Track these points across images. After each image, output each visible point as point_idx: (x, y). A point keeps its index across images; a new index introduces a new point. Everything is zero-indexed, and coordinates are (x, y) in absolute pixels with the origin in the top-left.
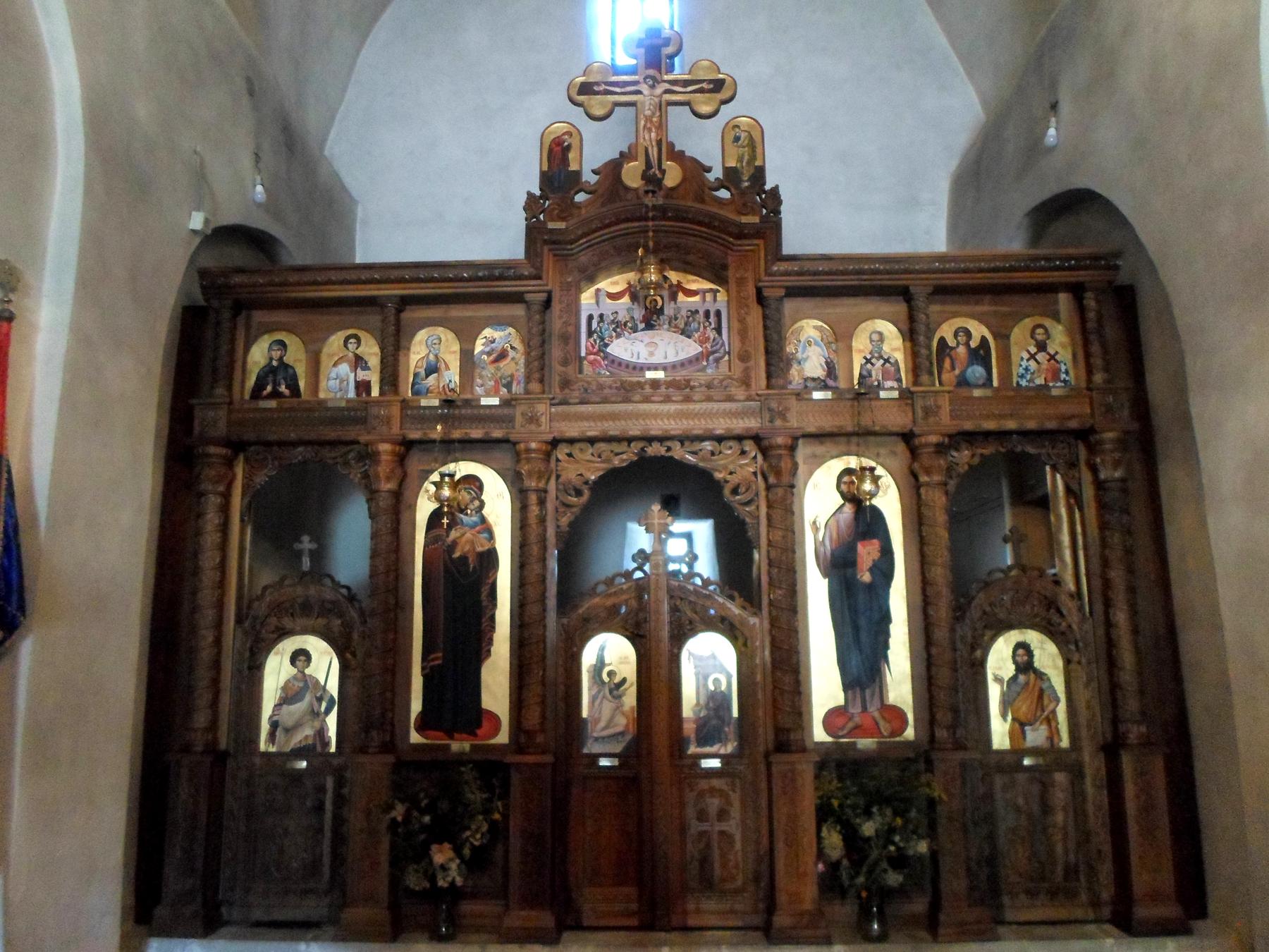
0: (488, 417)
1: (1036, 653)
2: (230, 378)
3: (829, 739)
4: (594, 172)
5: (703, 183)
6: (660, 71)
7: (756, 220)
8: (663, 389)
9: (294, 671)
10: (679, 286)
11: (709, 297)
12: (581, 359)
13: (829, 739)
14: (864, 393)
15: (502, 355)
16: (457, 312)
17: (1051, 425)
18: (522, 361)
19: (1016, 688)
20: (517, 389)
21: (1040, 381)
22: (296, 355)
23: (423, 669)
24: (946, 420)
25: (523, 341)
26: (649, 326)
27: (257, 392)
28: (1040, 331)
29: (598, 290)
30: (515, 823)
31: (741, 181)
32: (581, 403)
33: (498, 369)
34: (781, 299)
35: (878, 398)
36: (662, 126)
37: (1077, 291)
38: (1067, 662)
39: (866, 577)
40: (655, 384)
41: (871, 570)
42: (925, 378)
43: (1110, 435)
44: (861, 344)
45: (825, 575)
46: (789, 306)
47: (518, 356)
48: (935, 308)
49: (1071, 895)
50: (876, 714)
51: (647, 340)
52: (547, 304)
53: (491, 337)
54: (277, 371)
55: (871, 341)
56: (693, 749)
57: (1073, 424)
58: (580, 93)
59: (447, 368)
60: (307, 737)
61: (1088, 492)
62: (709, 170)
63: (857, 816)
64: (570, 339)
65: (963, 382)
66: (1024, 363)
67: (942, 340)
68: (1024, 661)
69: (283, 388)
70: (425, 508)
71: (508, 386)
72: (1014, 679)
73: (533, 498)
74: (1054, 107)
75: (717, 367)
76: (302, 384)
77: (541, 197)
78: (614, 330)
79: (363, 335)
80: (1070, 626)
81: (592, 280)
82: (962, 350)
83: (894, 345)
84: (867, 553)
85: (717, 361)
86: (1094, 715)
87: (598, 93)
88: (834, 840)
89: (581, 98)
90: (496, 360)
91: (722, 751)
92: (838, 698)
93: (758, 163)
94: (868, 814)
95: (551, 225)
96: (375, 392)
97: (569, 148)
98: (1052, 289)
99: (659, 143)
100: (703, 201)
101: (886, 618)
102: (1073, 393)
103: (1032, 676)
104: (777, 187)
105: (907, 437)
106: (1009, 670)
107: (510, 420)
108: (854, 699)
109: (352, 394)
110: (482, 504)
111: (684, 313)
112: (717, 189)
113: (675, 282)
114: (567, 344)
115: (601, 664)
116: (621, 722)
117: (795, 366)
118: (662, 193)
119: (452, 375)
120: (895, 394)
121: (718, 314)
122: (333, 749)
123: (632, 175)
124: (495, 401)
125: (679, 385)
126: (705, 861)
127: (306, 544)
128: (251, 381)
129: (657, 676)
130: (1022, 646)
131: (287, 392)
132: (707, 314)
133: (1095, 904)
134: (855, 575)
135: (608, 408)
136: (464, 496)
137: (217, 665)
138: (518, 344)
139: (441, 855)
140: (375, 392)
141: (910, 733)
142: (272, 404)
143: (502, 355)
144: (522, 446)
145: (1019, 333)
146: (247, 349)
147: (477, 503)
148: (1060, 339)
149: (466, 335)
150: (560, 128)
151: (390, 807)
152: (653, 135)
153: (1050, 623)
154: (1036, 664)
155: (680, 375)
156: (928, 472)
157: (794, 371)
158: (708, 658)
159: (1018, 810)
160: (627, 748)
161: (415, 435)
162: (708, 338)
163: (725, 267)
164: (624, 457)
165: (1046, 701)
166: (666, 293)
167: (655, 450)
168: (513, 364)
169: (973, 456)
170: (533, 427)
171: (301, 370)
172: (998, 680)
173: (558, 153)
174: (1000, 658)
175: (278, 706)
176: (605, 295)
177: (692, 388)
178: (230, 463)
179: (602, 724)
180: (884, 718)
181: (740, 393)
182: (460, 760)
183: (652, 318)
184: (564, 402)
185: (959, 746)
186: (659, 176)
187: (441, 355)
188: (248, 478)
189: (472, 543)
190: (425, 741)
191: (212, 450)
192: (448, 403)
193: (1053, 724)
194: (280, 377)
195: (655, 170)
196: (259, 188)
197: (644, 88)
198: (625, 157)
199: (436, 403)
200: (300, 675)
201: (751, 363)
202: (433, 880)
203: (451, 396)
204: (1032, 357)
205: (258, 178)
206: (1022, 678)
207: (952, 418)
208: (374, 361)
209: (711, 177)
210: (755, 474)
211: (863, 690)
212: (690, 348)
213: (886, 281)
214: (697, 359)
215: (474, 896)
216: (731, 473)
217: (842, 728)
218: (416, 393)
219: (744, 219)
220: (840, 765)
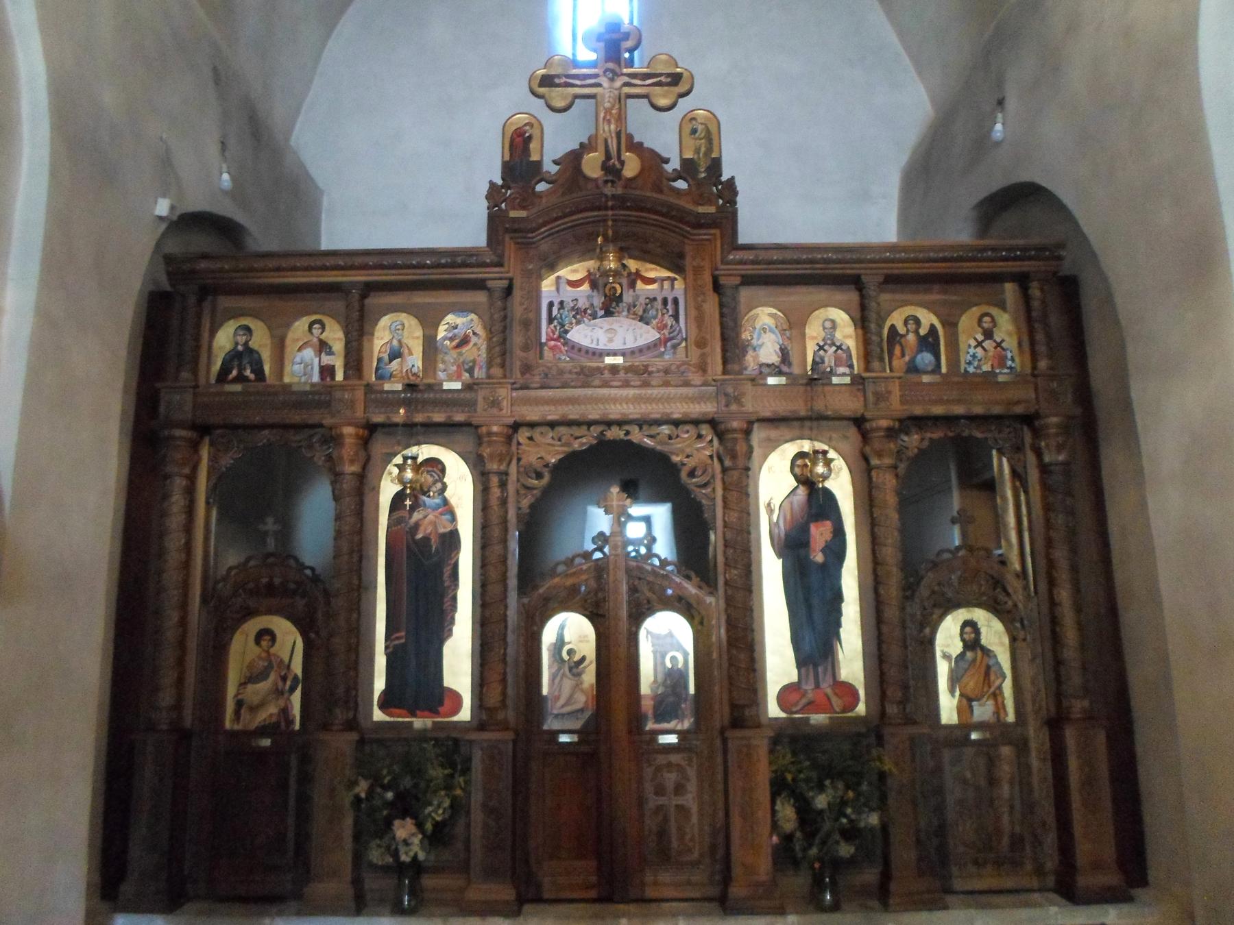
0: (450, 401)
1: (983, 631)
2: (195, 361)
3: (783, 715)
4: (555, 162)
5: (662, 172)
6: (619, 65)
7: (712, 210)
8: (622, 374)
9: (257, 650)
10: (638, 275)
11: (666, 285)
12: (541, 345)
13: (783, 715)
14: (816, 379)
15: (465, 341)
16: (421, 298)
17: (997, 410)
18: (484, 347)
19: (964, 665)
20: (479, 373)
21: (986, 368)
22: (261, 340)
23: (386, 648)
24: (896, 405)
25: (485, 328)
26: (608, 313)
27: (223, 376)
28: (986, 319)
29: (558, 278)
30: (477, 798)
31: (697, 171)
32: (542, 387)
33: (460, 354)
34: (737, 287)
35: (830, 384)
36: (621, 118)
37: (1022, 280)
38: (1013, 640)
39: (819, 558)
40: (614, 369)
41: (823, 551)
42: (876, 364)
43: (1054, 420)
44: (814, 331)
45: (779, 555)
46: (745, 294)
47: (480, 341)
48: (885, 297)
49: (1016, 864)
50: (829, 691)
51: (606, 327)
52: (509, 291)
53: (453, 323)
54: (243, 356)
55: (824, 328)
56: (650, 726)
57: (1019, 410)
58: (541, 84)
59: (411, 353)
60: (271, 715)
61: (1033, 475)
62: (667, 161)
63: (812, 789)
64: (530, 325)
65: (913, 368)
66: (972, 351)
67: (893, 327)
68: (972, 638)
69: (248, 373)
70: (388, 489)
71: (470, 371)
72: (961, 656)
73: (495, 480)
74: (1001, 102)
75: (674, 353)
76: (267, 368)
77: (502, 187)
78: (574, 317)
79: (328, 321)
80: (1015, 605)
81: (552, 267)
82: (911, 337)
83: (847, 333)
84: (820, 533)
85: (675, 347)
86: (1039, 691)
87: (558, 85)
88: (787, 813)
89: (542, 90)
90: (458, 346)
91: (679, 727)
92: (792, 675)
93: (714, 155)
94: (821, 788)
95: (513, 214)
96: (339, 377)
97: (530, 137)
98: (997, 278)
99: (618, 134)
100: (661, 192)
101: (838, 597)
102: (1019, 379)
103: (979, 653)
104: (733, 178)
105: (859, 422)
106: (957, 647)
107: (472, 404)
108: (807, 676)
109: (316, 378)
110: (444, 487)
111: (642, 300)
112: (674, 180)
113: (633, 270)
114: (528, 330)
115: (560, 643)
116: (581, 700)
117: (751, 353)
118: (621, 183)
119: (415, 360)
120: (847, 380)
121: (676, 301)
122: (297, 727)
123: (592, 165)
124: (457, 386)
125: (637, 371)
126: (662, 834)
127: (270, 525)
129: (616, 655)
130: (969, 624)
131: (252, 376)
132: (665, 301)
133: (1039, 871)
134: (807, 556)
135: (569, 392)
136: (426, 478)
137: (182, 644)
138: (479, 330)
139: (403, 829)
140: (339, 377)
141: (861, 708)
142: (238, 388)
143: (465, 341)
144: (484, 430)
145: (967, 321)
147: (439, 485)
148: (1006, 327)
149: (430, 322)
150: (521, 118)
151: (353, 784)
152: (613, 127)
153: (996, 601)
154: (983, 642)
155: (639, 361)
156: (880, 455)
157: (749, 358)
158: (666, 636)
159: (965, 782)
160: (585, 725)
161: (378, 418)
162: (665, 326)
163: (681, 256)
164: (584, 441)
165: (992, 677)
166: (625, 281)
167: (615, 433)
168: (475, 349)
169: (923, 439)
170: (495, 411)
171: (266, 355)
172: (946, 656)
173: (519, 144)
174: (948, 636)
175: (243, 684)
176: (564, 283)
177: (650, 373)
178: (195, 446)
179: (562, 701)
180: (836, 694)
181: (697, 379)
182: (423, 736)
184: (525, 387)
185: (909, 721)
186: (618, 166)
187: (405, 341)
188: (213, 459)
189: (434, 524)
190: (388, 719)
191: (178, 433)
192: (410, 387)
193: (1000, 699)
194: (245, 361)
195: (614, 161)
196: (226, 176)
197: (605, 82)
198: (584, 148)
199: (399, 387)
200: (264, 655)
201: (707, 350)
202: (396, 854)
203: (413, 380)
204: (979, 344)
205: (224, 166)
206: (969, 655)
207: (902, 403)
208: (338, 346)
209: (669, 168)
210: (711, 457)
211: (816, 666)
212: (648, 335)
213: (836, 270)
214: (654, 346)
215: (437, 870)
216: (688, 456)
217: (796, 704)
218: (380, 377)
219: (701, 210)
220: (794, 740)
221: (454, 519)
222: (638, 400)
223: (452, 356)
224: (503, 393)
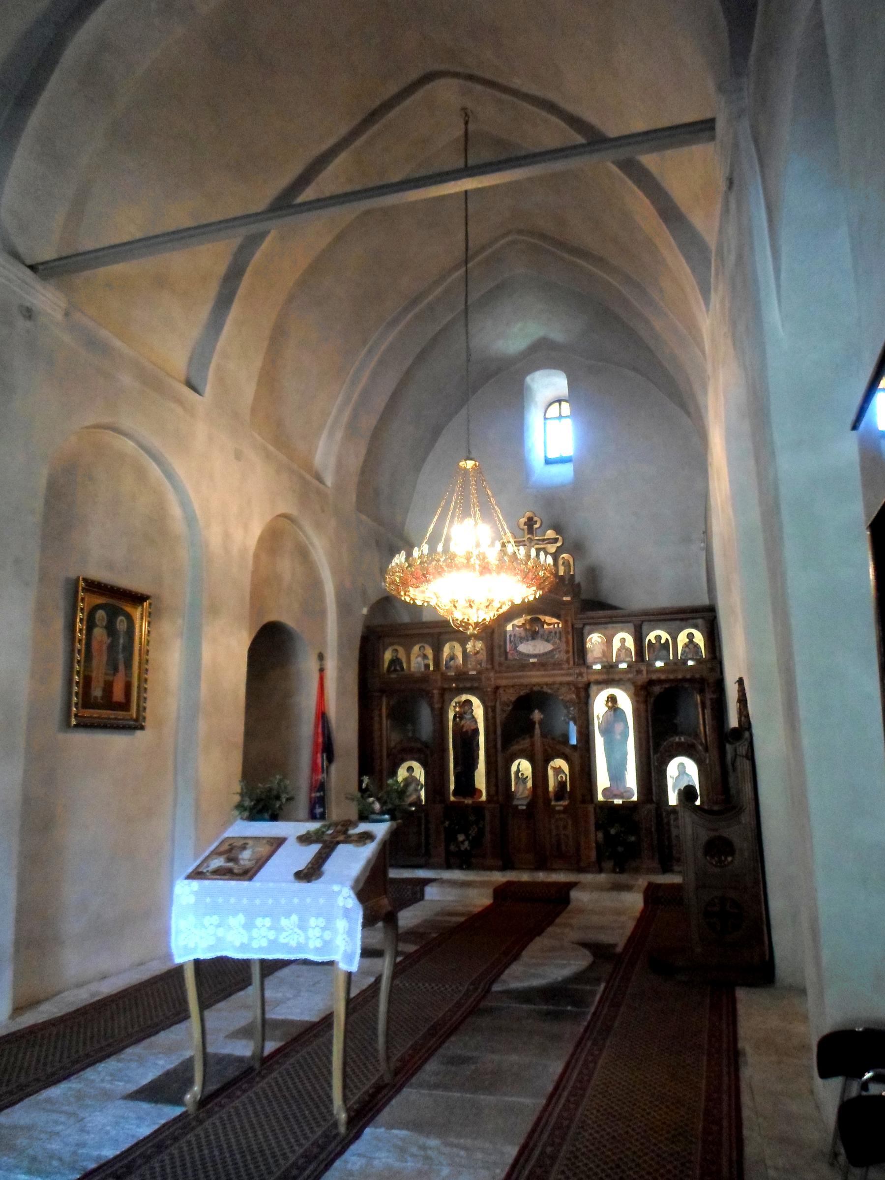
0: (472, 679)
10: (545, 622)
22: (402, 654)
26: (533, 638)
30: (488, 828)
40: (534, 663)
44: (616, 644)
69: (398, 668)
71: (480, 664)
73: (490, 709)
82: (658, 644)
83: (630, 643)
88: (600, 835)
96: (431, 668)
109: (423, 669)
115: (518, 771)
116: (527, 793)
119: (460, 660)
124: (474, 673)
125: (544, 663)
127: (409, 727)
128: (386, 665)
132: (556, 633)
135: (515, 674)
139: (461, 837)
140: (431, 668)
143: (478, 652)
146: (384, 653)
148: (699, 638)
151: (443, 822)
161: (446, 686)
171: (404, 660)
178: (380, 698)
182: (467, 806)
183: (534, 635)
184: (500, 672)
188: (388, 704)
202: (459, 847)
208: (431, 656)
218: (447, 668)
221: (476, 722)
222: (543, 676)
223: (473, 659)
224: (492, 674)
